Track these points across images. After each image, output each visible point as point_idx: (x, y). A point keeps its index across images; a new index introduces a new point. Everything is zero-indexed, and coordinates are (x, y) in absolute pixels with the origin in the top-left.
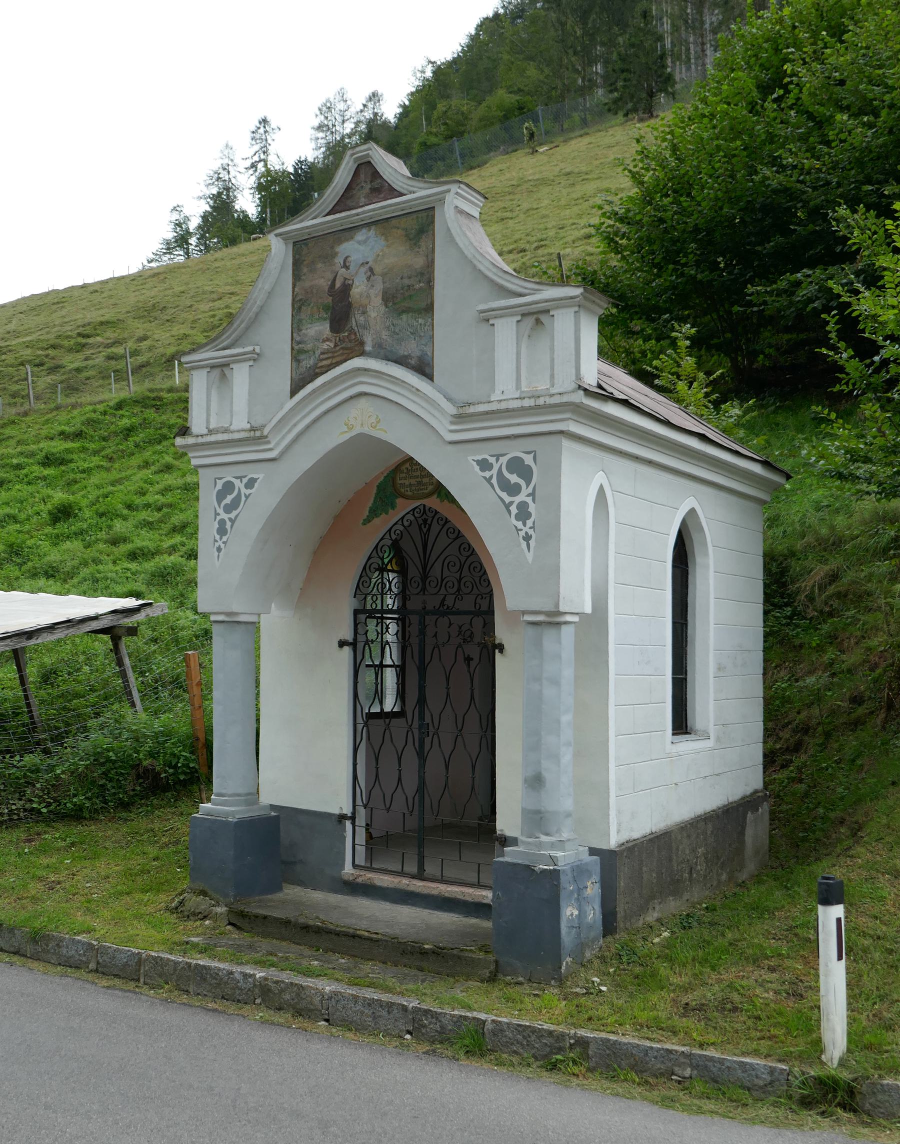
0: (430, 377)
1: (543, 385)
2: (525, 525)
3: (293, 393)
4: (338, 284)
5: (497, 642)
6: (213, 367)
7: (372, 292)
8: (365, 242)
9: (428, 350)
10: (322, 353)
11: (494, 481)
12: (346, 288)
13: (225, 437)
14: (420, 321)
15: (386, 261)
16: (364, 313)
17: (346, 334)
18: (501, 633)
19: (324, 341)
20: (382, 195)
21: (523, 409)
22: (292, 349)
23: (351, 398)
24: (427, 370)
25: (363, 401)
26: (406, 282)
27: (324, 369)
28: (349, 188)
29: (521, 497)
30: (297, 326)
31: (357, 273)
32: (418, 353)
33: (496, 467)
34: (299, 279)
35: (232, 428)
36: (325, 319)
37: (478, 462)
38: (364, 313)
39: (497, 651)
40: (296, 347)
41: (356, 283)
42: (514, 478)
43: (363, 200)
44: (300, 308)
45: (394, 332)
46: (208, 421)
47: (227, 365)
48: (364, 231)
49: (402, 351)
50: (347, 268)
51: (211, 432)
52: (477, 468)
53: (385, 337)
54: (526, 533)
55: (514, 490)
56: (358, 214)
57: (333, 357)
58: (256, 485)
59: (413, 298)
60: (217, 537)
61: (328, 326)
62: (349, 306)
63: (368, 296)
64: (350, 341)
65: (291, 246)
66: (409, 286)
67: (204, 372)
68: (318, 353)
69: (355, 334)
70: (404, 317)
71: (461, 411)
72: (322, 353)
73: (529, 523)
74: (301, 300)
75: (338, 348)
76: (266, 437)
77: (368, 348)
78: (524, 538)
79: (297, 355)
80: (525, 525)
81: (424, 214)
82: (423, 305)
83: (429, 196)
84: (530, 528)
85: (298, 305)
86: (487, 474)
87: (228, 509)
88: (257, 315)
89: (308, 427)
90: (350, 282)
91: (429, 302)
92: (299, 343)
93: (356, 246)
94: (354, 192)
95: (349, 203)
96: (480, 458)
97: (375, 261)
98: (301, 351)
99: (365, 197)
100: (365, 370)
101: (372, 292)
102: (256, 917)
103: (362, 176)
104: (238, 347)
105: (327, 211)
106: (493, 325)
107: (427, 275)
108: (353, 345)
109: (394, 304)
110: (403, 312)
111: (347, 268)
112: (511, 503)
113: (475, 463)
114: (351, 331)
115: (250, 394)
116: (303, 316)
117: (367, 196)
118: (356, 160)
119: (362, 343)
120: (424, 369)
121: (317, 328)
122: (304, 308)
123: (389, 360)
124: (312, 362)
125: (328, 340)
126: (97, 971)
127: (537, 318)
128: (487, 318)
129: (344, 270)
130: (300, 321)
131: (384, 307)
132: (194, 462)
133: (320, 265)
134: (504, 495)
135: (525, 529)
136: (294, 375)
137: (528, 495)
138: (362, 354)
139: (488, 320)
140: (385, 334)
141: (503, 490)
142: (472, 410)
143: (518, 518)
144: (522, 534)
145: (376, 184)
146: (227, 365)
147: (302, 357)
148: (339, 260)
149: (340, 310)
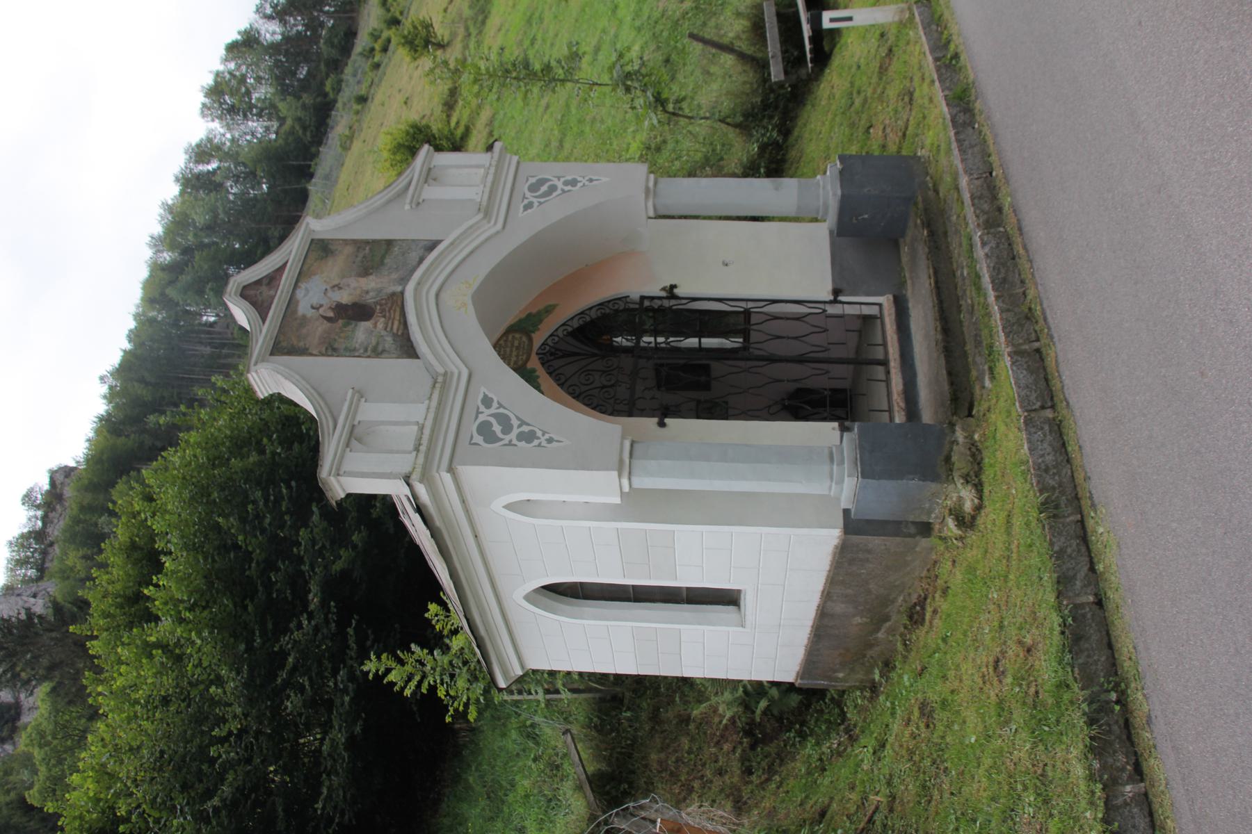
4: (331, 314)
13: (427, 432)
38: (367, 292)
43: (272, 292)
44: (334, 350)
48: (298, 292)
50: (321, 306)
58: (490, 395)
62: (355, 305)
63: (355, 289)
68: (383, 333)
77: (399, 289)
92: (366, 350)
103: (252, 292)
111: (321, 306)
114: (376, 303)
119: (393, 294)
122: (336, 346)
124: (389, 339)
126: (1053, 407)
133: (304, 331)
145: (265, 282)
147: (380, 349)
148: (310, 313)
149: (357, 312)
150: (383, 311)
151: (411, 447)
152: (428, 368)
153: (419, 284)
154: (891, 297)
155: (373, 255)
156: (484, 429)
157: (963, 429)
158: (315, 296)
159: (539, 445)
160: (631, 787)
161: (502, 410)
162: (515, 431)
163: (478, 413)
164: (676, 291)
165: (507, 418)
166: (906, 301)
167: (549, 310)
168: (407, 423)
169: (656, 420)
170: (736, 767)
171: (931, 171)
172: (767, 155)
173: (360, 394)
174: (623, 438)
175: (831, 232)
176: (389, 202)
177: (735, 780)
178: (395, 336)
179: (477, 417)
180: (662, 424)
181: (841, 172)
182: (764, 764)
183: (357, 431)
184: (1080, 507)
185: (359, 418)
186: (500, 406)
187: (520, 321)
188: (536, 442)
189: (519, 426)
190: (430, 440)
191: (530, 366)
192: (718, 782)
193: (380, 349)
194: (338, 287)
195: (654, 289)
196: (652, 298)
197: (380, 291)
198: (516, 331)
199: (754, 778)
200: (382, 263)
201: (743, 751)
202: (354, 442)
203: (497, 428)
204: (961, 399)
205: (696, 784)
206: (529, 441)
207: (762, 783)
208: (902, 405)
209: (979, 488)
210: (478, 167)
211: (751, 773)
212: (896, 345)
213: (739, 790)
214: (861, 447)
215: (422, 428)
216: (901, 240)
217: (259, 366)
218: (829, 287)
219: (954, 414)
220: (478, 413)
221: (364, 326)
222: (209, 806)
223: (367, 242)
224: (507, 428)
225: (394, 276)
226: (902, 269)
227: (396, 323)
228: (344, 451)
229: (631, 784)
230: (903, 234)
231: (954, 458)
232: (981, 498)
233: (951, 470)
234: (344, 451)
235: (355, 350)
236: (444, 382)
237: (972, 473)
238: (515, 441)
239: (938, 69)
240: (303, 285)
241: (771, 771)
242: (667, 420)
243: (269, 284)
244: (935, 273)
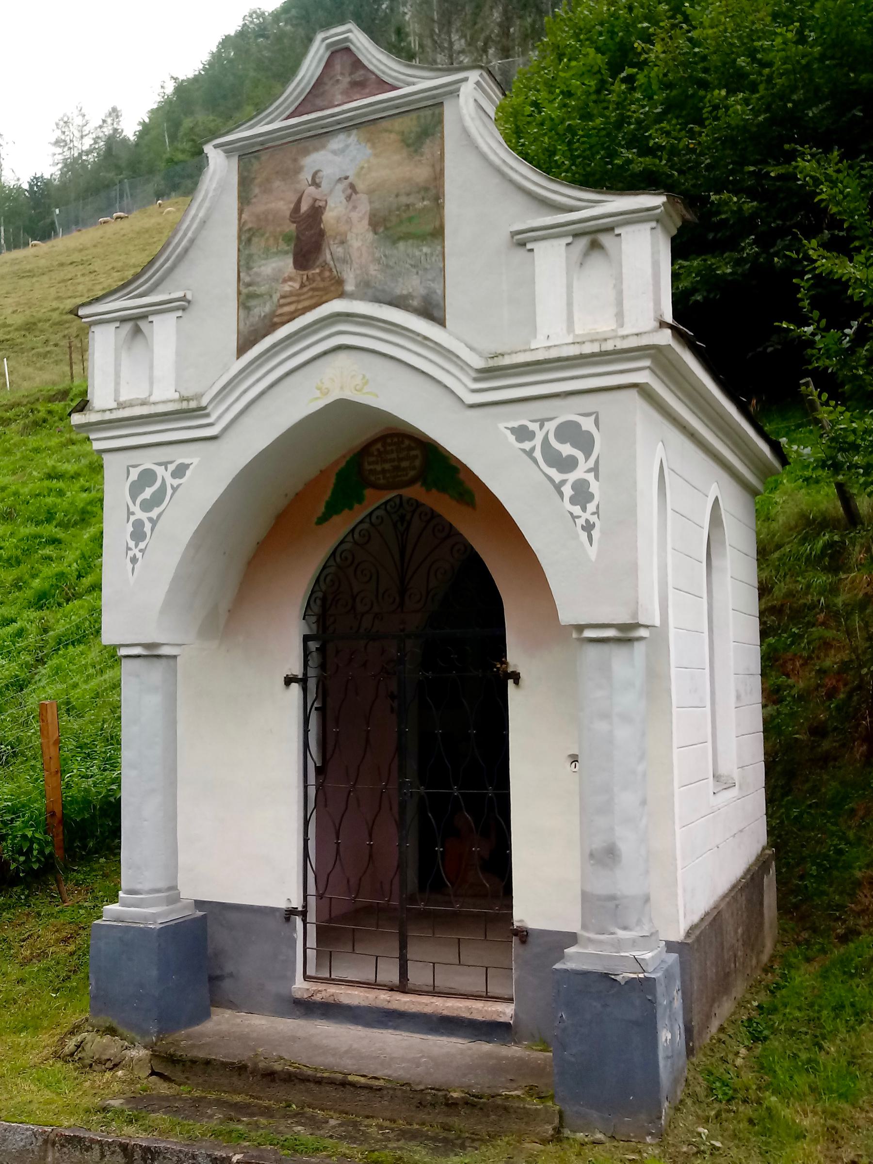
0: (441, 322)
1: (605, 325)
2: (584, 509)
3: (241, 350)
4: (304, 207)
5: (510, 670)
6: (124, 320)
7: (355, 216)
8: (342, 151)
9: (437, 287)
10: (283, 297)
11: (538, 454)
12: (316, 212)
14: (425, 249)
15: (374, 174)
16: (342, 242)
17: (317, 271)
18: (516, 656)
19: (285, 281)
20: (367, 91)
21: (582, 356)
22: (239, 293)
23: (325, 353)
24: (436, 313)
25: (342, 358)
26: (404, 200)
27: (285, 318)
28: (319, 82)
29: (578, 474)
30: (245, 263)
31: (331, 191)
32: (422, 291)
35: (153, 399)
36: (286, 253)
37: (513, 430)
39: (510, 682)
40: (244, 291)
41: (331, 203)
42: (566, 450)
43: (339, 98)
44: (249, 240)
45: (387, 266)
46: (117, 392)
47: (144, 316)
48: (342, 136)
49: (400, 289)
51: (121, 406)
52: (512, 438)
53: (373, 273)
54: (587, 521)
56: (333, 115)
57: (298, 302)
59: (414, 221)
60: (132, 544)
61: (289, 261)
62: (321, 234)
63: (349, 221)
64: (323, 280)
65: (235, 161)
66: (408, 206)
67: (112, 327)
68: (276, 297)
69: (331, 270)
70: (401, 245)
71: (491, 363)
72: (283, 297)
73: (591, 507)
74: (250, 229)
75: (305, 289)
76: (205, 408)
77: (349, 287)
78: (583, 528)
79: (245, 300)
80: (584, 509)
81: (428, 112)
82: (429, 228)
84: (593, 514)
85: (247, 236)
86: (527, 445)
87: (147, 506)
88: (186, 250)
89: (263, 393)
90: (322, 204)
91: (437, 224)
92: (249, 285)
93: (330, 157)
94: (327, 88)
95: (319, 102)
96: (515, 424)
97: (358, 175)
98: (251, 296)
99: (342, 93)
100: (348, 315)
101: (355, 216)
102: (194, 1062)
103: (338, 68)
105: (287, 113)
106: (532, 250)
107: (434, 192)
108: (327, 283)
109: (386, 229)
110: (400, 238)
112: (564, 482)
113: (508, 432)
114: (325, 266)
115: (178, 354)
116: (254, 249)
117: (345, 93)
119: (340, 282)
120: (432, 310)
121: (274, 265)
122: (255, 240)
123: (380, 302)
124: (267, 309)
125: (291, 279)
127: (594, 238)
128: (522, 241)
129: (312, 188)
130: (250, 256)
131: (370, 236)
132: (97, 446)
133: (277, 184)
134: (553, 472)
135: (587, 515)
137: (589, 471)
138: (342, 295)
139: (524, 245)
140: (373, 270)
141: (550, 465)
142: (507, 361)
143: (573, 501)
144: (581, 522)
145: (358, 76)
146: (144, 316)
147: (252, 303)
148: (306, 176)
149: (308, 241)
156: (148, 477)
159: (129, 549)
161: (169, 491)
163: (165, 464)
165: (158, 504)
178: (273, 314)
179: (160, 464)
186: (175, 489)
197: (345, 260)
200: (395, 241)
202: (128, 327)
203: (148, 493)
220: (165, 464)
221: (287, 264)
227: (292, 308)
235: (249, 268)
236: (194, 410)
240: (353, 138)
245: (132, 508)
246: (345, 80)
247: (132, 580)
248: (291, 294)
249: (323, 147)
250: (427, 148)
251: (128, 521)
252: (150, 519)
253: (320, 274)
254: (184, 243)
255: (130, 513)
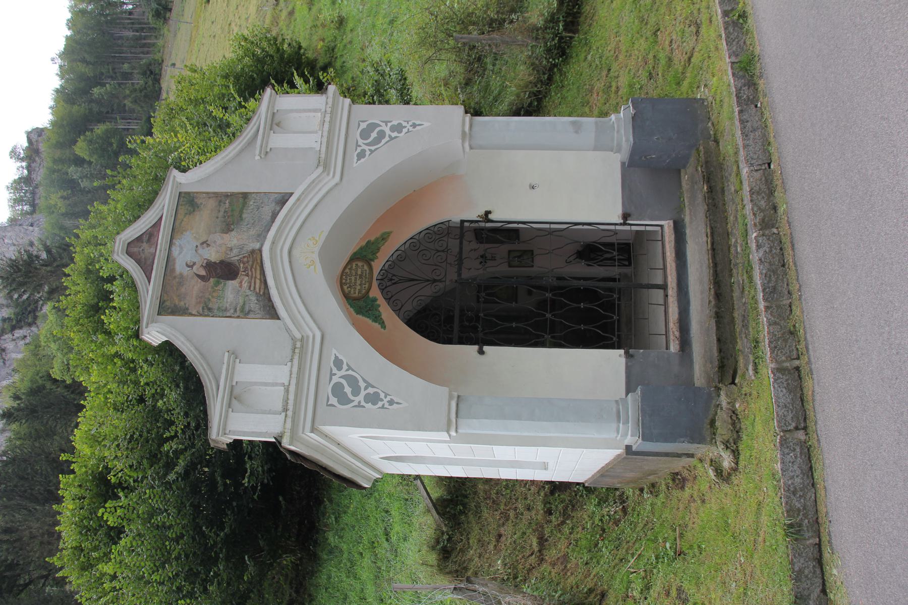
4: (203, 273)
7: (219, 242)
8: (181, 247)
12: (210, 267)
19: (241, 286)
22: (238, 317)
23: (290, 262)
25: (295, 252)
26: (221, 214)
27: (263, 287)
28: (138, 262)
30: (223, 313)
31: (201, 256)
33: (364, 147)
34: (187, 309)
36: (225, 285)
40: (238, 313)
41: (207, 256)
43: (152, 250)
44: (210, 309)
48: (173, 249)
50: (194, 264)
55: (382, 134)
61: (231, 282)
64: (248, 262)
66: (225, 212)
74: (203, 309)
77: (257, 246)
79: (244, 313)
83: (171, 192)
85: (207, 311)
92: (235, 311)
93: (181, 256)
95: (149, 262)
98: (242, 310)
101: (219, 242)
103: (136, 250)
104: (221, 373)
108: (251, 260)
111: (194, 264)
114: (240, 261)
116: (215, 307)
118: (122, 253)
119: (253, 252)
124: (253, 298)
125: (241, 282)
129: (195, 267)
130: (219, 309)
131: (233, 233)
133: (183, 290)
136: (259, 316)
138: (260, 250)
140: (252, 232)
145: (145, 238)
147: (247, 309)
148: (186, 271)
149: (224, 270)
150: (246, 269)
151: (279, 406)
152: (288, 330)
153: (273, 243)
154: (671, 222)
155: (234, 208)
156: (338, 390)
157: (727, 395)
158: (189, 253)
159: (383, 407)
160: (465, 507)
161: (350, 372)
162: (363, 393)
164: (491, 217)
166: (684, 227)
167: (384, 238)
168: (276, 384)
169: (476, 347)
170: (540, 506)
171: (713, 118)
172: (565, 9)
173: (234, 354)
174: (451, 398)
175: (623, 164)
176: (242, 151)
177: (540, 517)
178: (258, 294)
179: (331, 379)
180: (481, 352)
181: (634, 118)
182: (560, 507)
183: (237, 391)
184: (819, 531)
185: (235, 380)
186: (349, 368)
187: (361, 248)
188: (380, 404)
189: (366, 388)
190: (295, 405)
191: (372, 295)
192: (527, 515)
193: (247, 309)
194: (205, 243)
195: (473, 214)
196: (472, 222)
198: (358, 259)
199: (553, 518)
200: (241, 218)
201: (546, 495)
203: (348, 390)
204: (726, 369)
205: (512, 514)
206: (374, 404)
207: (559, 525)
208: (677, 334)
209: (736, 454)
210: (315, 111)
211: (551, 514)
212: (674, 273)
213: (542, 527)
214: (643, 411)
215: (287, 391)
216: (682, 171)
217: (150, 329)
218: (619, 211)
219: (721, 381)
220: (332, 375)
221: (232, 284)
222: (172, 477)
223: (227, 195)
224: (356, 391)
225: (252, 232)
226: (682, 193)
227: (258, 282)
228: (227, 411)
229: (464, 505)
230: (684, 167)
231: (718, 424)
232: (737, 463)
233: (714, 434)
234: (227, 411)
235: (226, 310)
236: (302, 346)
237: (731, 440)
238: (363, 403)
239: (726, 26)
240: (177, 242)
241: (566, 515)
242: (486, 348)
243: (149, 241)
244: (712, 234)
245: (356, 403)
246: (145, 245)
247: (405, 404)
248: (250, 283)
249: (174, 260)
250: (198, 201)
251: (364, 407)
252: (366, 388)
253: (244, 264)
254: (196, 353)
255: (359, 405)
